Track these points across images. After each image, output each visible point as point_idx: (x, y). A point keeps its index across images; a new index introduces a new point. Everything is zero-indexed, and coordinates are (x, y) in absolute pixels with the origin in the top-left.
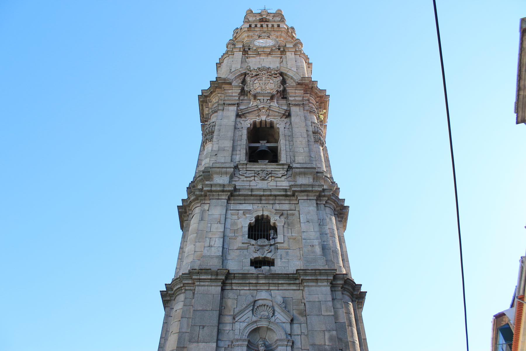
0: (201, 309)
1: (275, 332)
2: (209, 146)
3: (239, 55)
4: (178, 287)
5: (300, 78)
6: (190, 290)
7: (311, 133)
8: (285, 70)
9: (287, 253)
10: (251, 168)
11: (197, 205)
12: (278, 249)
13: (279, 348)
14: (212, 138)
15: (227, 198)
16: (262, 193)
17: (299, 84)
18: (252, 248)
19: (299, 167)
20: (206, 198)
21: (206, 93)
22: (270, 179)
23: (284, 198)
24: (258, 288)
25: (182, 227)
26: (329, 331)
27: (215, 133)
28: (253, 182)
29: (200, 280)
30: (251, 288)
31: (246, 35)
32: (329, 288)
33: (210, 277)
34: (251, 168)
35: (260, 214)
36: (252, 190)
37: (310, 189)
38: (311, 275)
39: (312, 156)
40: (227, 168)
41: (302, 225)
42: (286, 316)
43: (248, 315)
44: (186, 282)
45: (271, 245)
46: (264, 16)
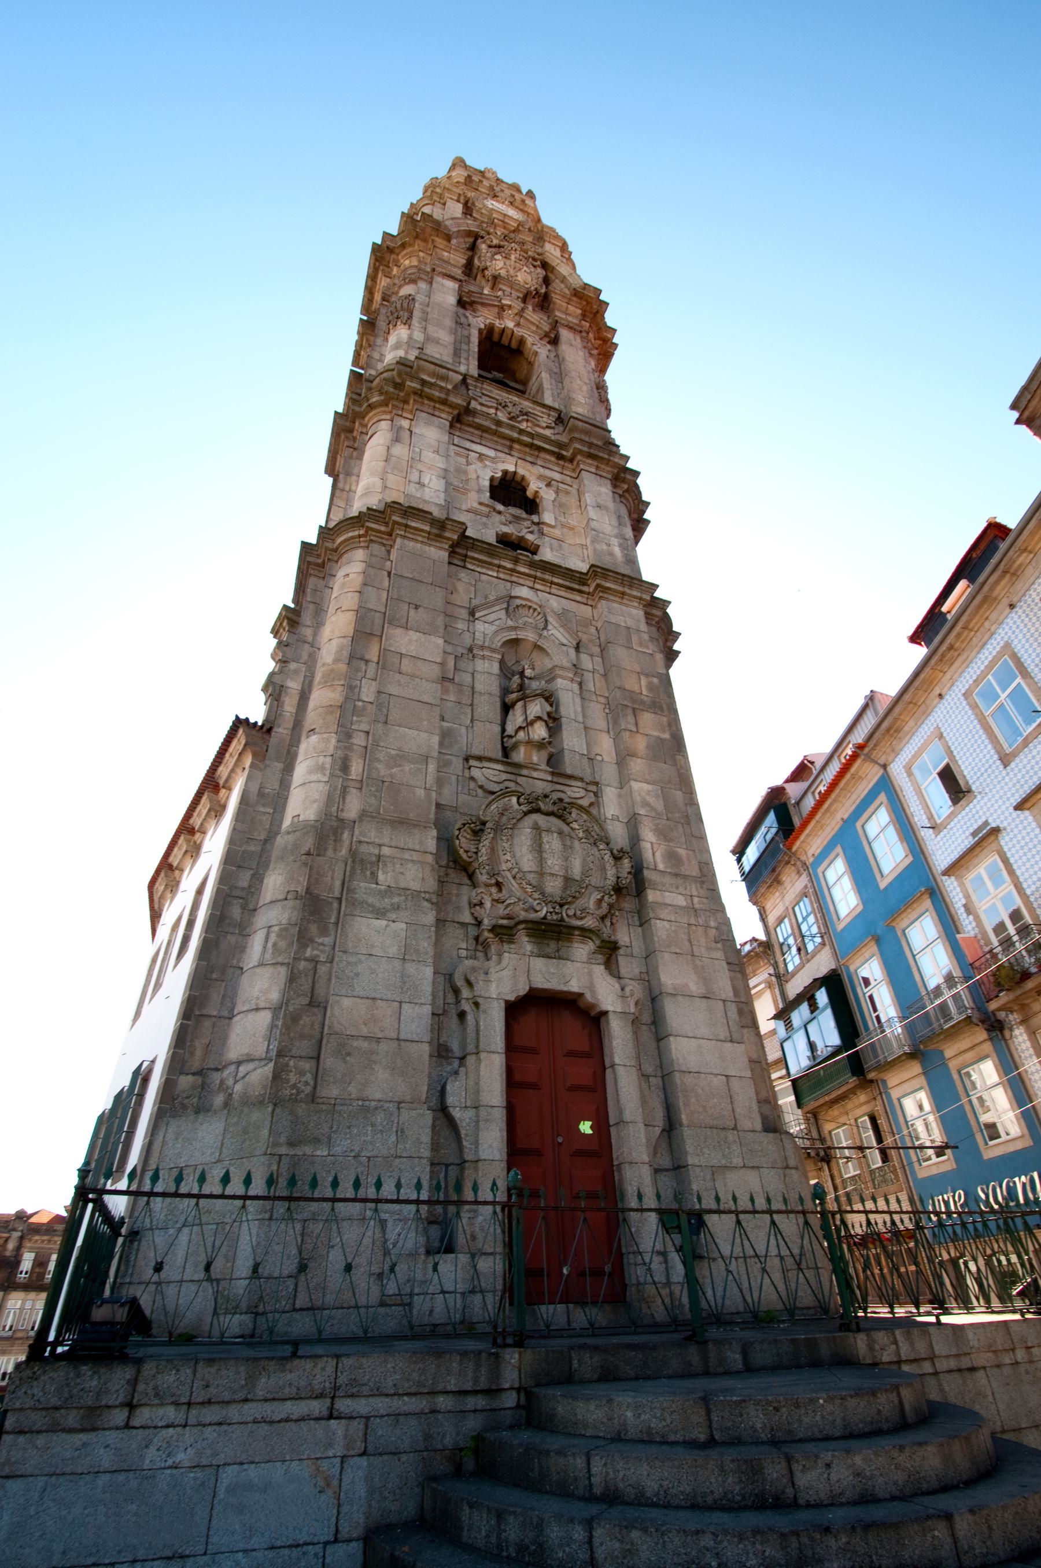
0: (411, 576)
1: (548, 654)
4: (350, 534)
6: (384, 545)
10: (491, 391)
11: (384, 417)
13: (559, 681)
14: (410, 318)
15: (450, 419)
16: (515, 435)
18: (497, 518)
20: (406, 407)
23: (553, 459)
24: (514, 579)
25: (331, 469)
30: (501, 576)
32: (642, 613)
33: (427, 528)
34: (491, 391)
40: (449, 369)
42: (567, 636)
43: (498, 614)
45: (533, 523)
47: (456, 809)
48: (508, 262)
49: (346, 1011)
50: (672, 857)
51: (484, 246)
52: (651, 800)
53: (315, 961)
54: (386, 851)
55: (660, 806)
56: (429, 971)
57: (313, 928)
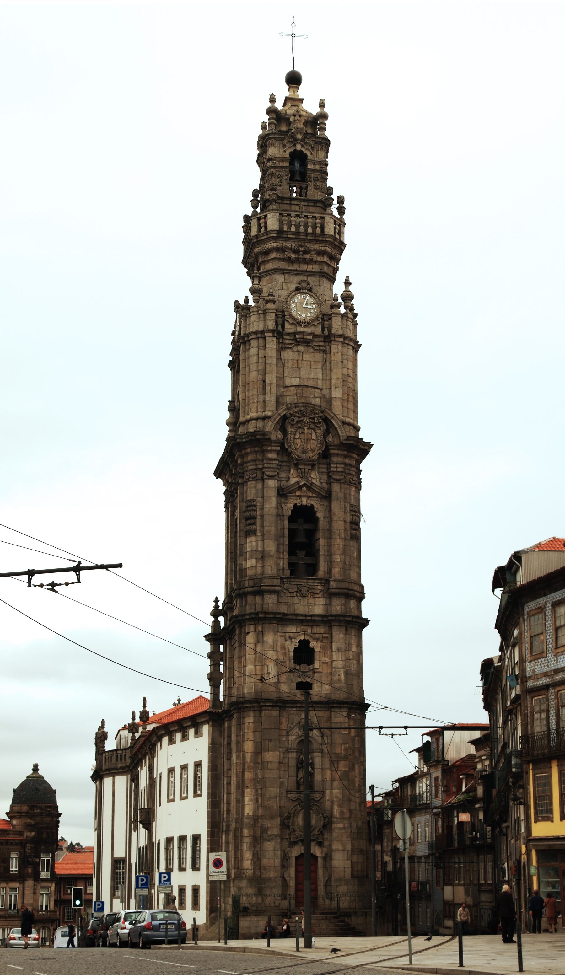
0: (268, 727)
3: (272, 343)
4: (248, 705)
8: (330, 416)
9: (321, 677)
11: (251, 623)
12: (314, 672)
14: (256, 530)
16: (304, 618)
17: (342, 443)
19: (335, 587)
21: (240, 439)
26: (344, 744)
27: (258, 521)
28: (296, 598)
29: (265, 706)
31: (274, 245)
35: (302, 638)
36: (297, 615)
37: (342, 619)
38: (337, 703)
39: (347, 563)
40: (275, 586)
41: (333, 653)
44: (254, 705)
46: (299, 147)
47: (285, 807)
48: (302, 436)
49: (265, 862)
50: (342, 813)
52: (338, 795)
53: (257, 851)
54: (269, 825)
55: (340, 797)
56: (279, 852)
57: (256, 844)
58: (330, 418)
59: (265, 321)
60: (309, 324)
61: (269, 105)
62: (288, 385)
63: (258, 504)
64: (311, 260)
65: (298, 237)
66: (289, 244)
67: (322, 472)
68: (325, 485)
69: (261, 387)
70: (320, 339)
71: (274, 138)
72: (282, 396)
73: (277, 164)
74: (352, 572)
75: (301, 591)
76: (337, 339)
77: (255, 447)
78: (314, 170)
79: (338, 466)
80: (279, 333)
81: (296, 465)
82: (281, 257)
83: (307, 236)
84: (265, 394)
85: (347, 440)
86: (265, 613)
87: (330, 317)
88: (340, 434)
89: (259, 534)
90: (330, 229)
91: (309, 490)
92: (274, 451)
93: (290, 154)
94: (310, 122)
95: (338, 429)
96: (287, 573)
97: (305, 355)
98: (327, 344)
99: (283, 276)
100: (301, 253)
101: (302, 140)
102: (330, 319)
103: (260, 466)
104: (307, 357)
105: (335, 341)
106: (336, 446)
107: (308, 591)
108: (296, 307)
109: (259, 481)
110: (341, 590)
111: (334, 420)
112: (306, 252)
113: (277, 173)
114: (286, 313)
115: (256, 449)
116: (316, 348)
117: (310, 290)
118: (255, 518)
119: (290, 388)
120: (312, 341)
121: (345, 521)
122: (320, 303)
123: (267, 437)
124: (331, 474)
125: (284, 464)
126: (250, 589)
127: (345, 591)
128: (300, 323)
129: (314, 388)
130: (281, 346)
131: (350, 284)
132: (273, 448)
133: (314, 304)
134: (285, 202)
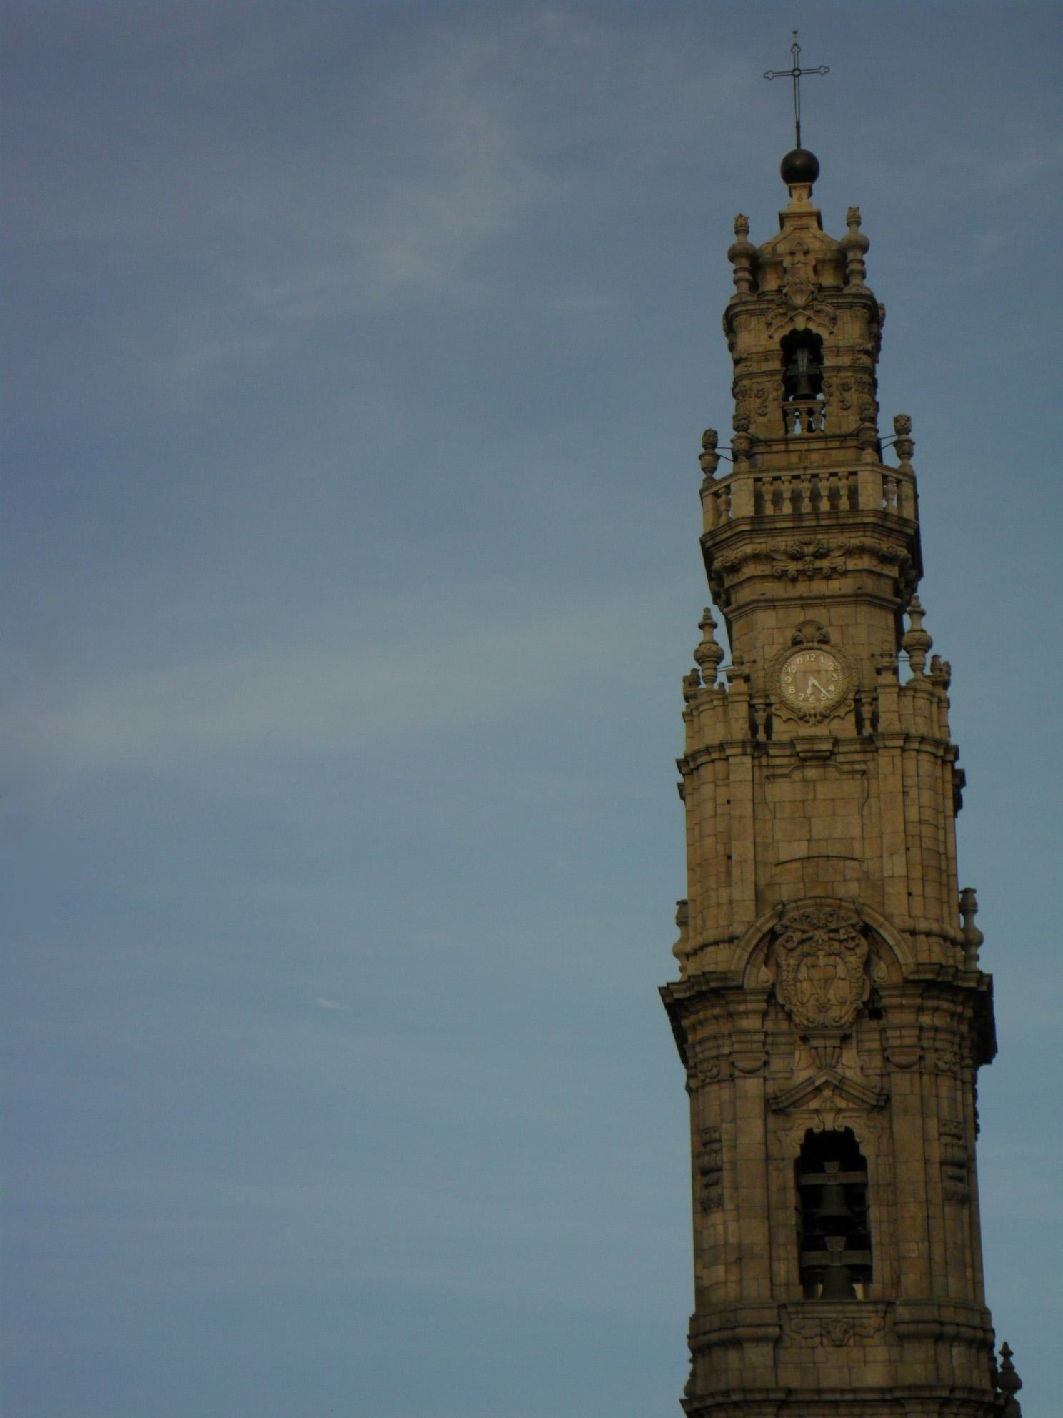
2: (717, 1217)
3: (742, 767)
5: (912, 967)
7: (935, 1171)
8: (875, 920)
14: (721, 1197)
16: (838, 1397)
17: (907, 981)
19: (907, 1317)
21: (679, 991)
22: (851, 1342)
27: (727, 1176)
31: (748, 549)
36: (820, 1391)
37: (926, 1394)
39: (937, 1259)
46: (800, 324)
51: (782, 952)
58: (874, 925)
59: (727, 722)
60: (825, 717)
61: (733, 240)
62: (782, 859)
63: (724, 1137)
64: (834, 570)
65: (797, 524)
66: (783, 543)
67: (870, 1051)
68: (875, 1081)
69: (723, 869)
70: (853, 748)
71: (747, 312)
72: (771, 885)
73: (755, 368)
74: (951, 1281)
75: (829, 1332)
76: (889, 743)
77: (713, 1007)
78: (839, 369)
79: (905, 1032)
80: (757, 747)
81: (805, 1039)
82: (767, 573)
83: (818, 519)
84: (729, 885)
85: (917, 972)
86: (744, 1391)
87: (874, 695)
88: (902, 961)
89: (729, 1205)
90: (870, 497)
91: (840, 1096)
92: (755, 1012)
93: (785, 342)
94: (830, 261)
95: (896, 949)
96: (797, 1292)
97: (819, 789)
98: (869, 756)
99: (772, 614)
100: (808, 559)
101: (805, 308)
102: (875, 699)
103: (726, 1050)
104: (823, 791)
105: (885, 747)
106: (895, 987)
107: (846, 1332)
108: (794, 682)
109: (727, 1084)
110: (921, 1326)
111: (885, 929)
112: (819, 555)
113: (755, 387)
114: (773, 699)
115: (717, 1011)
116: (846, 768)
117: (824, 641)
118: (720, 1169)
119: (789, 866)
120: (832, 753)
121: (927, 1161)
122: (846, 668)
123: (733, 984)
124: (887, 1054)
125: (782, 1039)
126: (714, 1337)
127: (935, 1328)
128: (803, 718)
129: (845, 858)
130: (766, 772)
131: (923, 613)
132: (750, 1006)
133: (835, 670)
134: (775, 448)
